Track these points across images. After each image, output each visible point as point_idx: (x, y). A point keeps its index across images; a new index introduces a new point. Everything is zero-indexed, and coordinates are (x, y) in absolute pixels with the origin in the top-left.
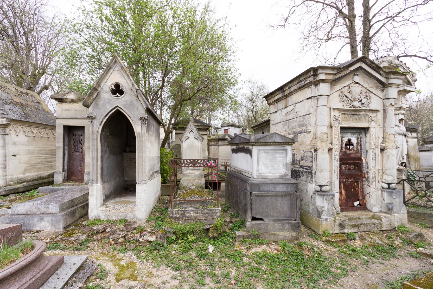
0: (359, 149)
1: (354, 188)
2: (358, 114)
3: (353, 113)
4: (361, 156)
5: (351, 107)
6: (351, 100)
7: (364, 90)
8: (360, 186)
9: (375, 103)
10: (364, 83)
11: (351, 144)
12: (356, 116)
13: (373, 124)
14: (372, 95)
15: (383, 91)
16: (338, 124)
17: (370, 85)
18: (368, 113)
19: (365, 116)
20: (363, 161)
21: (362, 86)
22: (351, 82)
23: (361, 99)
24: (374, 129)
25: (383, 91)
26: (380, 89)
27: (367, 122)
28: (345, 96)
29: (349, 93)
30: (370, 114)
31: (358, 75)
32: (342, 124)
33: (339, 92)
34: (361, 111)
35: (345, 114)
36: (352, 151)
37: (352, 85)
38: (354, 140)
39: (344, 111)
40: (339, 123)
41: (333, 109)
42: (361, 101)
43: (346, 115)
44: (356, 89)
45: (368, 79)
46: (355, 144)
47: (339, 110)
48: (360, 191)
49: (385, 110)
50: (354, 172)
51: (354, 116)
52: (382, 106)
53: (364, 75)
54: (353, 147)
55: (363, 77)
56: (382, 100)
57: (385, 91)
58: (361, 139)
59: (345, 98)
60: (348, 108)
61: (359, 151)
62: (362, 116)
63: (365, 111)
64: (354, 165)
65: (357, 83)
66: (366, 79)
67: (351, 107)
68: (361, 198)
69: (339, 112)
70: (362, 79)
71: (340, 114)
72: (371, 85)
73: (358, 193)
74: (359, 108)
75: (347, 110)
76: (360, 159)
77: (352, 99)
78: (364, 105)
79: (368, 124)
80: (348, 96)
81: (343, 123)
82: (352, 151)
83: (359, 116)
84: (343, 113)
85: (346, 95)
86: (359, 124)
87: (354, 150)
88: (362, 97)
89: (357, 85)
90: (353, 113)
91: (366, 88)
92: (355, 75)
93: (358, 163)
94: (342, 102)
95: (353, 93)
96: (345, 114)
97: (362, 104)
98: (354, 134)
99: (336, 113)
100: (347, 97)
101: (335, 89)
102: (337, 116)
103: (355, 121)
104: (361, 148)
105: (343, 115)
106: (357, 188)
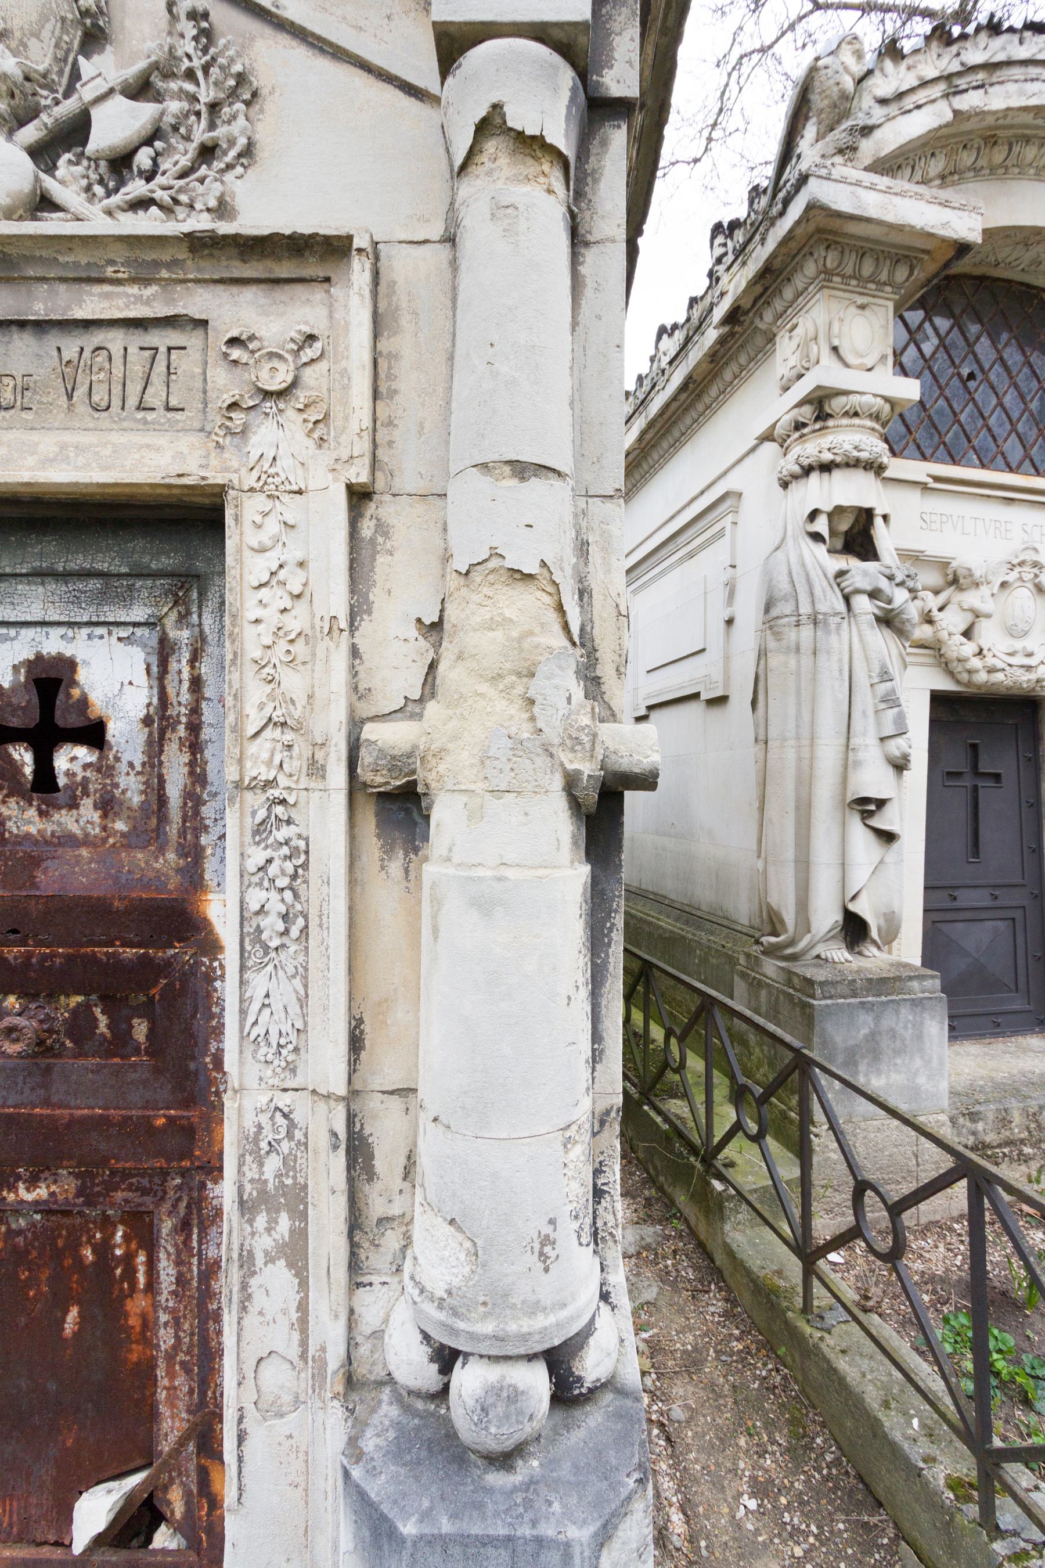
0: (174, 792)
1: (106, 1290)
4: (194, 878)
8: (167, 1272)
11: (64, 719)
13: (277, 437)
19: (160, 339)
20: (212, 947)
24: (291, 509)
36: (88, 811)
38: (114, 678)
42: (75, 132)
46: (125, 732)
48: (166, 1338)
50: (83, 1092)
54: (105, 769)
58: (194, 660)
61: (176, 823)
62: (115, 340)
63: (145, 259)
64: (110, 1002)
68: (172, 1425)
73: (146, 1373)
76: (177, 920)
78: (136, 188)
82: (88, 811)
87: (108, 805)
93: (147, 971)
97: (120, 163)
98: (103, 597)
104: (198, 775)
106: (138, 1304)
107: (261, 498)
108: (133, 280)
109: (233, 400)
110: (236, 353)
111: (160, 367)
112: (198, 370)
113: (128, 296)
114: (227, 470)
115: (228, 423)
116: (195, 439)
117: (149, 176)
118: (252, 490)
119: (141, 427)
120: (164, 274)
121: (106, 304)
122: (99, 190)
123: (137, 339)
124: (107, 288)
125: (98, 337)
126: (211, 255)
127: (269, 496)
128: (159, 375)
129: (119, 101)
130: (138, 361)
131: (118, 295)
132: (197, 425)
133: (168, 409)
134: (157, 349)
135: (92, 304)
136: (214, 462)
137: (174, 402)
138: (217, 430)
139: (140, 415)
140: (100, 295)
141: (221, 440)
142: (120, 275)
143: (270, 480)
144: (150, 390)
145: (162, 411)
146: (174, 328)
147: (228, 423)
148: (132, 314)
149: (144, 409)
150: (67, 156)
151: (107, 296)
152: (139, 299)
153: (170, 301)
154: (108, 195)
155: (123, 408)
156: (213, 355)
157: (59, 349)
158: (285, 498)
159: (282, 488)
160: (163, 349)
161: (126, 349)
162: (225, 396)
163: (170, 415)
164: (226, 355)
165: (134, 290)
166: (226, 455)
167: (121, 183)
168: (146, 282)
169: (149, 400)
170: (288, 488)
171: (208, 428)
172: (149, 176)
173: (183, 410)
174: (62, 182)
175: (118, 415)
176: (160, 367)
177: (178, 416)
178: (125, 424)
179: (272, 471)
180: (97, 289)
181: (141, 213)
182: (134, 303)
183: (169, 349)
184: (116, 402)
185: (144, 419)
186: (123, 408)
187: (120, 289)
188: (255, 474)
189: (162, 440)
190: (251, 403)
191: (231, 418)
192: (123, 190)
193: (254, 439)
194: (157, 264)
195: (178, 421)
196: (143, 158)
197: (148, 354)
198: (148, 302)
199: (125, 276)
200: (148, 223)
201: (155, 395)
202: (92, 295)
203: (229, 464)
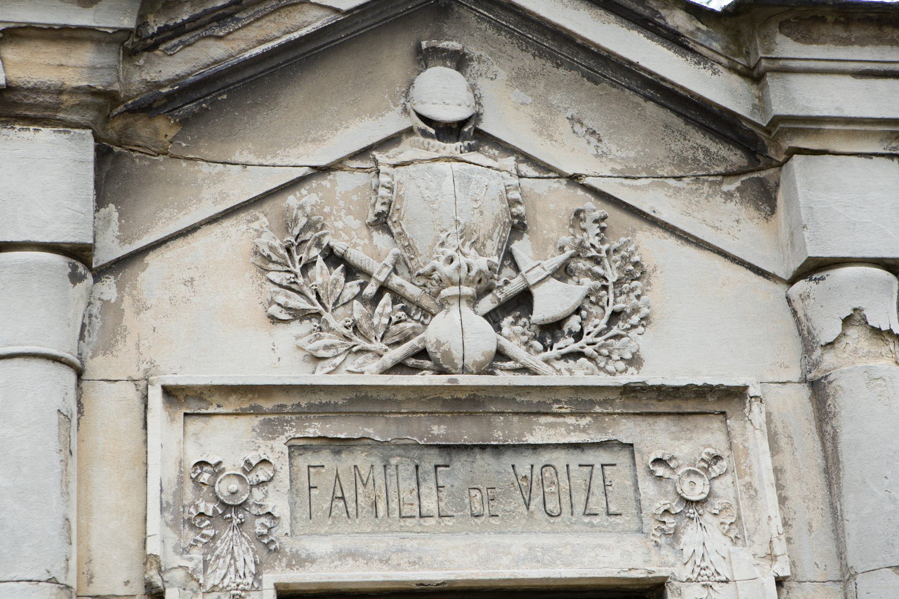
2: (498, 436)
3: (439, 431)
5: (399, 367)
6: (397, 297)
7: (552, 202)
9: (699, 316)
10: (543, 128)
12: (484, 462)
13: (702, 538)
14: (650, 246)
15: (765, 198)
16: (246, 554)
17: (608, 145)
18: (624, 430)
21: (528, 159)
22: (393, 123)
23: (516, 285)
25: (765, 198)
26: (732, 186)
27: (627, 520)
28: (332, 258)
29: (381, 222)
30: (655, 437)
31: (460, 61)
32: (298, 561)
33: (262, 218)
34: (538, 402)
35: (339, 445)
37: (407, 151)
39: (324, 412)
40: (268, 547)
41: (169, 392)
42: (523, 301)
43: (360, 459)
44: (449, 196)
45: (569, 95)
47: (248, 396)
49: (818, 388)
51: (461, 465)
52: (792, 347)
53: (528, 61)
55: (520, 79)
56: (780, 290)
57: (781, 198)
59: (323, 275)
60: (368, 373)
62: (560, 459)
63: (582, 399)
65: (448, 131)
66: (556, 98)
67: (399, 367)
69: (270, 430)
70: (518, 95)
71: (276, 449)
72: (624, 150)
74: (503, 378)
75: (361, 400)
77: (412, 291)
78: (568, 344)
79: (632, 542)
80: (357, 256)
81: (319, 546)
83: (524, 464)
84: (314, 429)
85: (339, 246)
86: (518, 544)
88: (534, 260)
89: (452, 148)
90: (439, 431)
91: (574, 179)
92: (425, 58)
94: (301, 315)
95: (414, 219)
96: (339, 445)
97: (552, 329)
99: (228, 441)
100: (351, 271)
101: (206, 193)
102: (234, 464)
103: (485, 510)
105: (325, 458)
107: (697, 586)
108: (572, 414)
109: (666, 507)
110: (660, 471)
111: (597, 481)
112: (629, 483)
113: (568, 425)
114: (663, 564)
115: (664, 527)
116: (637, 539)
117: (578, 336)
118: (689, 580)
119: (588, 529)
120: (598, 409)
121: (552, 432)
122: (538, 345)
123: (575, 459)
124: (550, 419)
125: (546, 457)
126: (636, 397)
127: (704, 586)
128: (598, 487)
129: (554, 284)
130: (579, 476)
131: (560, 424)
132: (636, 528)
133: (609, 514)
134: (592, 466)
135: (541, 432)
136: (655, 558)
137: (613, 509)
138: (654, 532)
139: (587, 520)
140: (546, 425)
141: (658, 540)
142: (563, 410)
143: (703, 572)
144: (592, 499)
145: (604, 516)
146: (605, 450)
147: (664, 527)
148: (574, 439)
149: (589, 515)
150: (510, 319)
151: (552, 425)
152: (577, 428)
153: (602, 430)
154: (545, 350)
155: (572, 514)
156: (641, 471)
157: (513, 466)
158: (716, 586)
159: (712, 578)
160: (598, 466)
161: (567, 466)
162: (658, 505)
163: (613, 519)
164: (652, 472)
165: (571, 420)
166: (663, 552)
167: (555, 339)
168: (582, 415)
169: (593, 507)
170: (718, 578)
171: (645, 530)
172: (578, 336)
173: (620, 514)
174: (508, 338)
175: (570, 520)
176: (597, 481)
177: (618, 520)
178: (575, 527)
179: (703, 565)
180: (543, 420)
181: (571, 362)
182: (574, 431)
183: (602, 466)
184: (566, 509)
185: (590, 522)
186: (572, 514)
187: (561, 420)
188: (690, 566)
189: (609, 540)
190: (678, 511)
191: (664, 522)
192: (556, 346)
193: (684, 539)
194: (592, 403)
195: (618, 524)
196: (574, 323)
197: (587, 470)
198: (584, 430)
199: (568, 411)
200: (581, 374)
201: (597, 503)
202: (540, 425)
203: (666, 559)
